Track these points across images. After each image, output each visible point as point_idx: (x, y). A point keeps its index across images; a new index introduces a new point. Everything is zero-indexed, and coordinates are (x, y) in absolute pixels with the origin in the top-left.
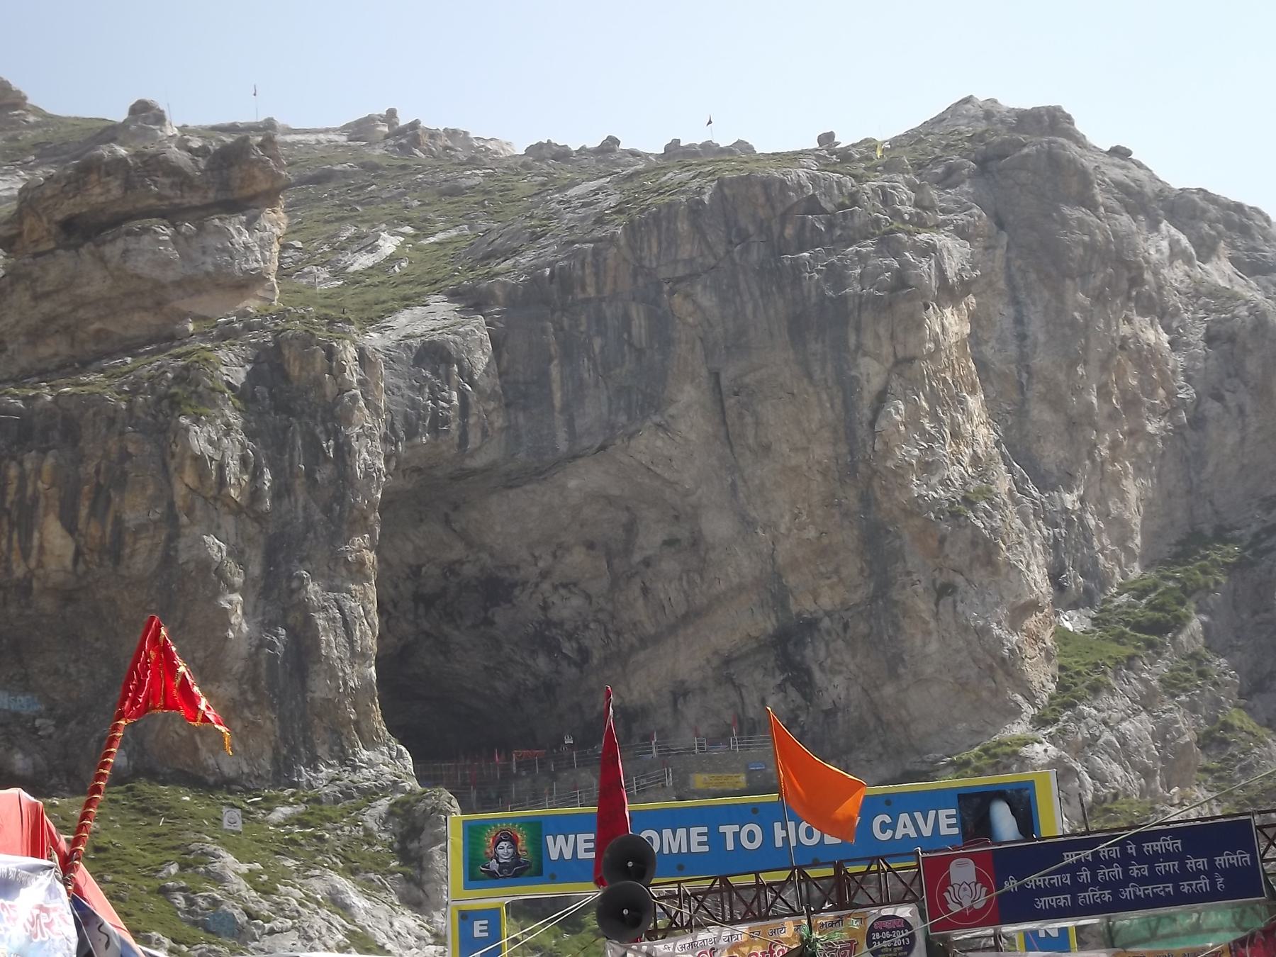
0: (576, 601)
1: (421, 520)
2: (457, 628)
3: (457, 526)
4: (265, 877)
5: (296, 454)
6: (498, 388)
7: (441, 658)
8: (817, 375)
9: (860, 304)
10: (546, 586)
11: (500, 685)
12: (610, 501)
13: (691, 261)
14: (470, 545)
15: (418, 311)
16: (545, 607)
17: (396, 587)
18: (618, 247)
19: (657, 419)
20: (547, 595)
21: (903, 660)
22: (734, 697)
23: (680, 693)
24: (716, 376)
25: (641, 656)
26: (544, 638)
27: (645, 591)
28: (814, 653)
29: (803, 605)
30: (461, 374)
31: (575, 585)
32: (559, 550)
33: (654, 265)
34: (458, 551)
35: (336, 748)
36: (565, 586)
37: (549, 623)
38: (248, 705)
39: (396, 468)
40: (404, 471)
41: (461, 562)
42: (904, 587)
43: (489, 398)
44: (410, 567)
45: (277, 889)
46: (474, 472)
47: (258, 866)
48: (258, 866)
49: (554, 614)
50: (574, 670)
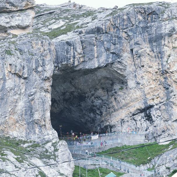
0: (100, 101)
1: (65, 82)
2: (73, 107)
3: (73, 84)
4: (21, 159)
5: (33, 64)
6: (82, 52)
7: (69, 113)
8: (155, 51)
9: (165, 35)
10: (93, 98)
11: (82, 120)
12: (107, 78)
13: (127, 25)
14: (76, 88)
15: (65, 35)
16: (93, 102)
17: (59, 97)
18: (111, 22)
19: (118, 60)
20: (93, 99)
21: (173, 115)
22: (134, 123)
23: (123, 121)
24: (132, 50)
25: (114, 113)
26: (92, 110)
27: (115, 99)
28: (154, 113)
29: (151, 103)
30: (73, 49)
31: (99, 97)
32: (96, 90)
33: (118, 26)
34: (73, 89)
35: (40, 131)
36: (97, 98)
37: (94, 106)
38: (20, 120)
39: (58, 69)
40: (60, 70)
41: (74, 92)
42: (173, 98)
43: (80, 54)
44: (62, 93)
45: (23, 162)
46: (76, 71)
47: (19, 156)
48: (19, 156)
49: (94, 104)
50: (99, 117)
